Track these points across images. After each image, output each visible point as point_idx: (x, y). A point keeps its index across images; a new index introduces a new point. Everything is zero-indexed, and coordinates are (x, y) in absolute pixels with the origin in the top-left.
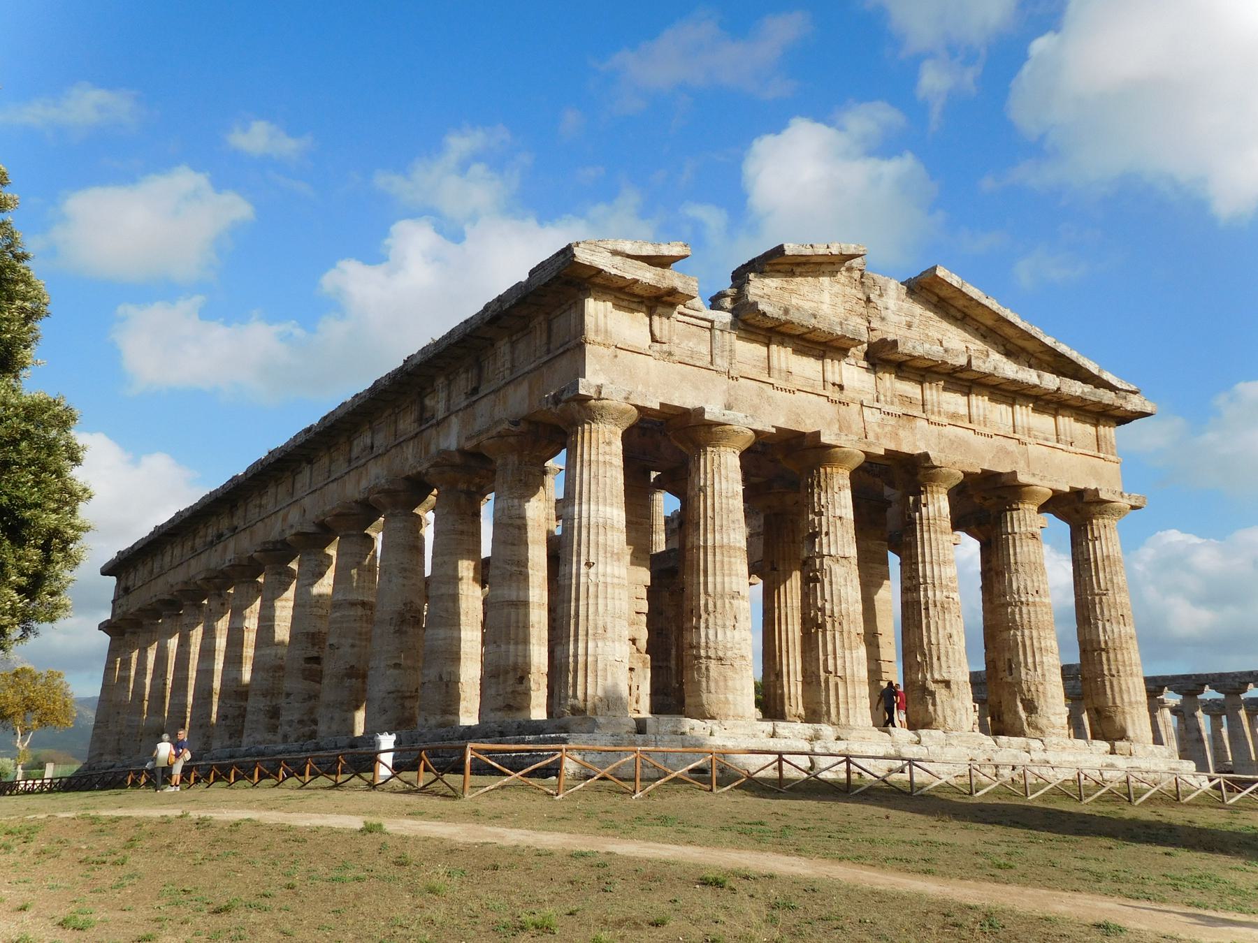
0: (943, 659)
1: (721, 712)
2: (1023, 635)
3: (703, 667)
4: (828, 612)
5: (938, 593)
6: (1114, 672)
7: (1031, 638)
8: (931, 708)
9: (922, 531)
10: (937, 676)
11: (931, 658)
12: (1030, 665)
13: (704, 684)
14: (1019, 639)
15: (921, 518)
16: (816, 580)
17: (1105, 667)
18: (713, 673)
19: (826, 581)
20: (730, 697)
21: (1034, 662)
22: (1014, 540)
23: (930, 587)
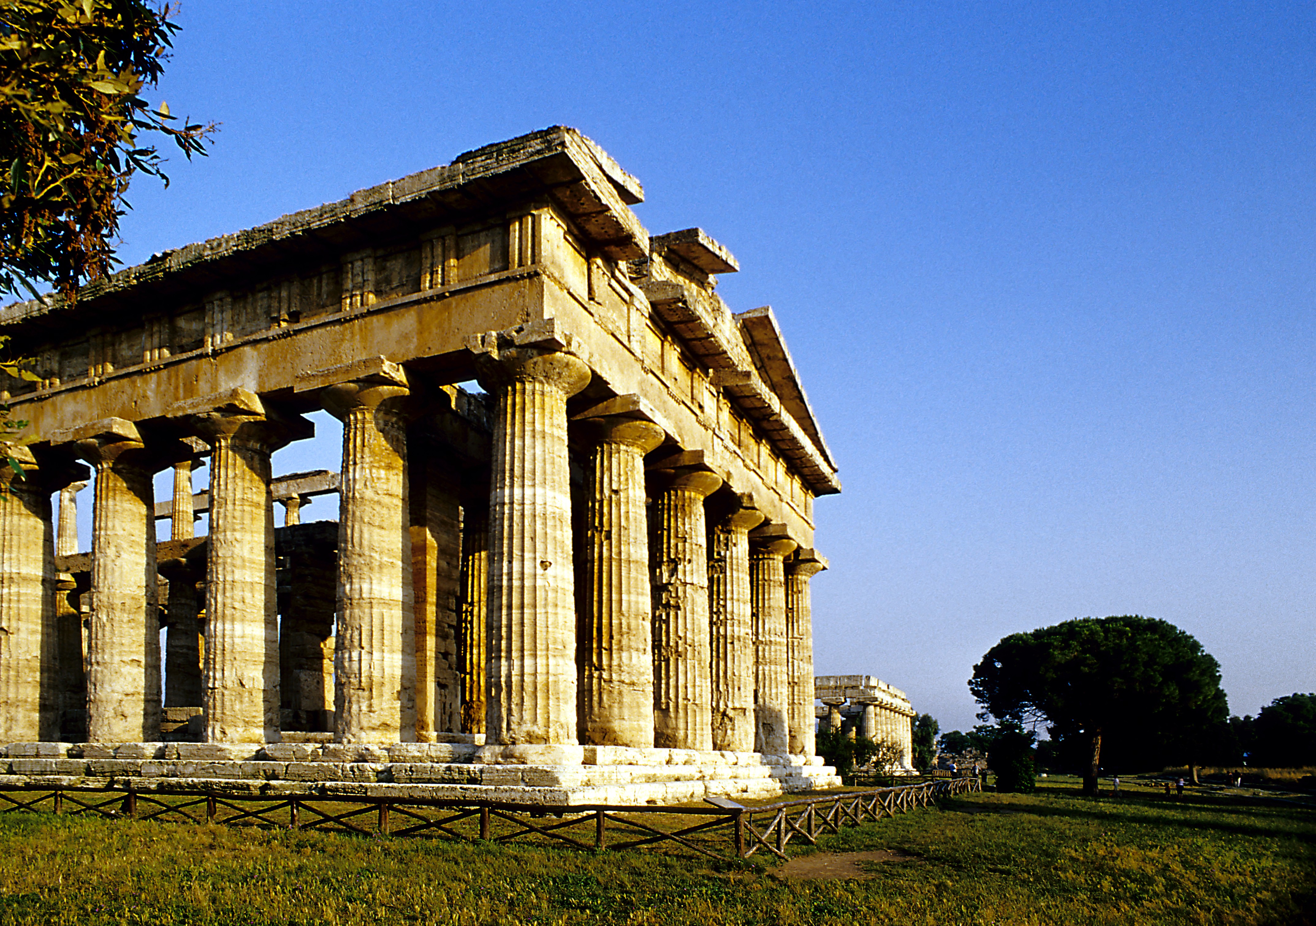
0: (742, 689)
1: (634, 739)
2: (770, 670)
3: (616, 692)
4: (689, 641)
5: (742, 629)
6: (802, 702)
7: (776, 673)
8: (729, 732)
9: (732, 569)
10: (737, 705)
11: (733, 688)
12: (773, 696)
13: (616, 711)
14: (767, 673)
15: (731, 557)
16: (678, 608)
17: (796, 697)
18: (626, 700)
19: (688, 609)
20: (642, 723)
21: (777, 694)
22: (769, 585)
23: (736, 622)
